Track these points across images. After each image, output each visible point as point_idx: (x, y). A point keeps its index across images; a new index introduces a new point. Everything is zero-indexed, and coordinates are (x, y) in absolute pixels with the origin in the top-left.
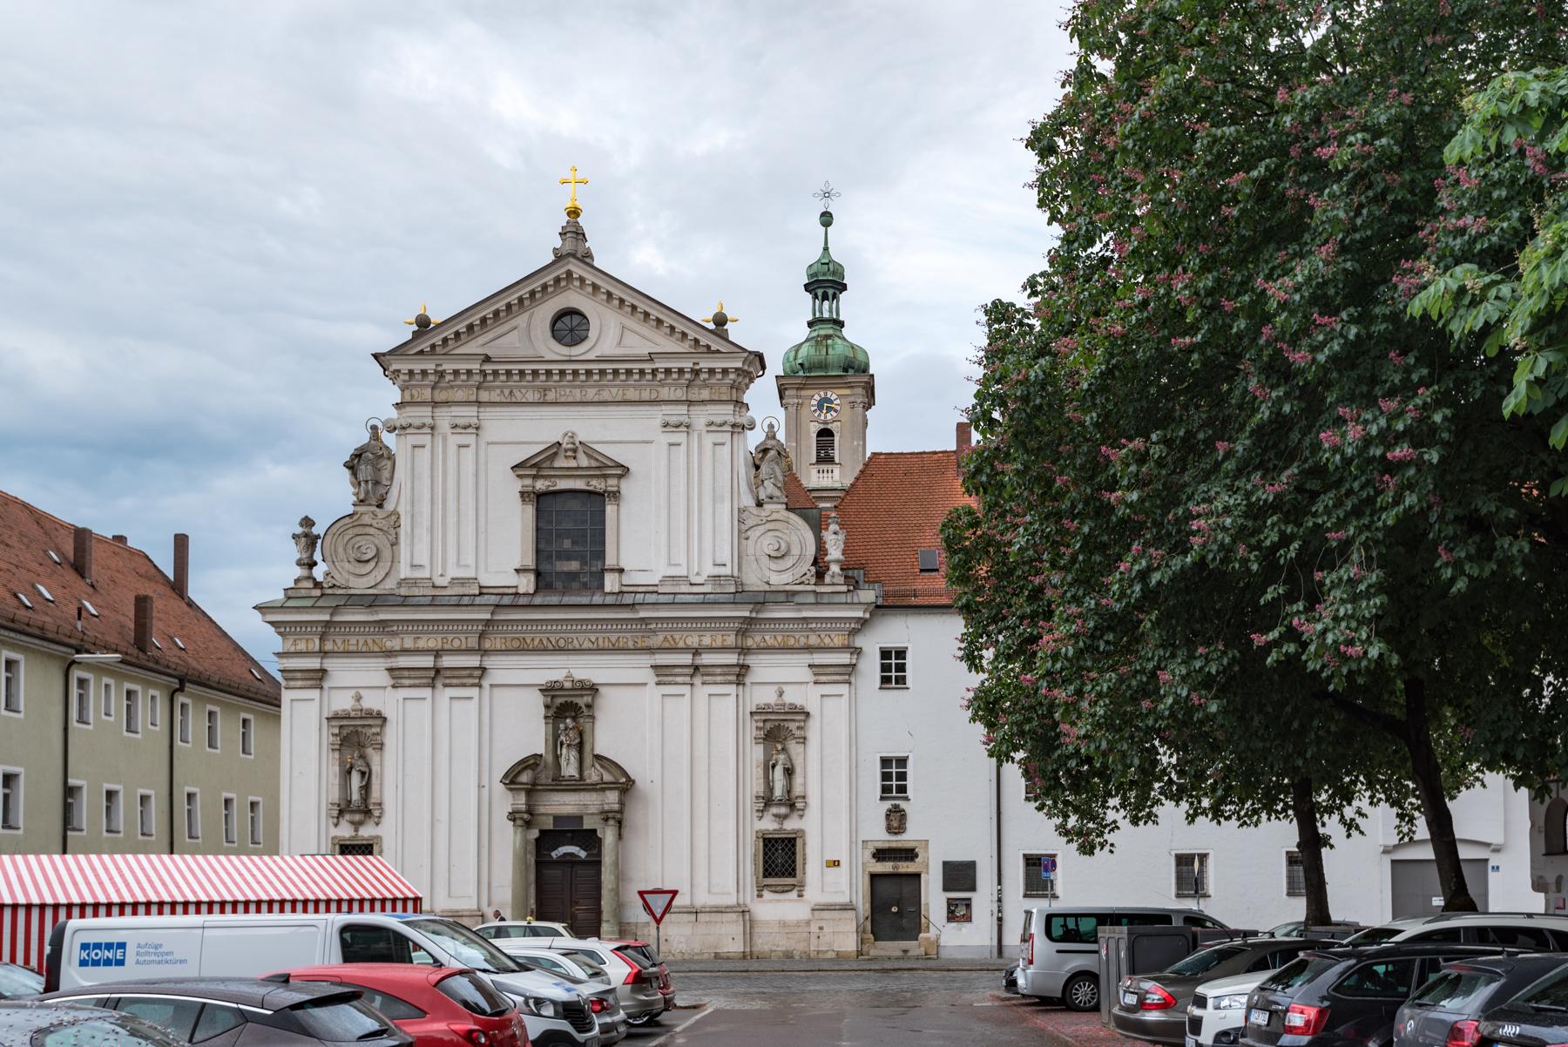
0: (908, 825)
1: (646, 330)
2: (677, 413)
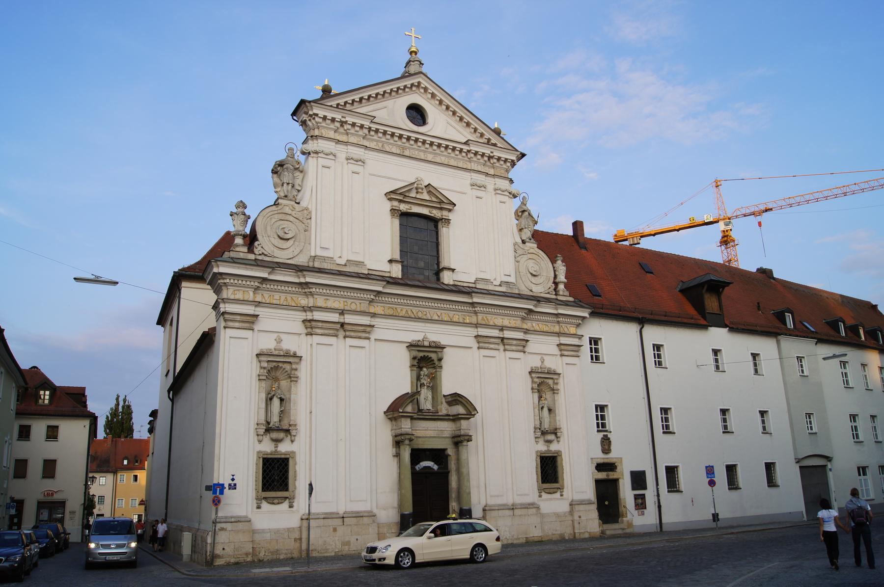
0: (612, 448)
1: (460, 127)
2: (480, 179)
